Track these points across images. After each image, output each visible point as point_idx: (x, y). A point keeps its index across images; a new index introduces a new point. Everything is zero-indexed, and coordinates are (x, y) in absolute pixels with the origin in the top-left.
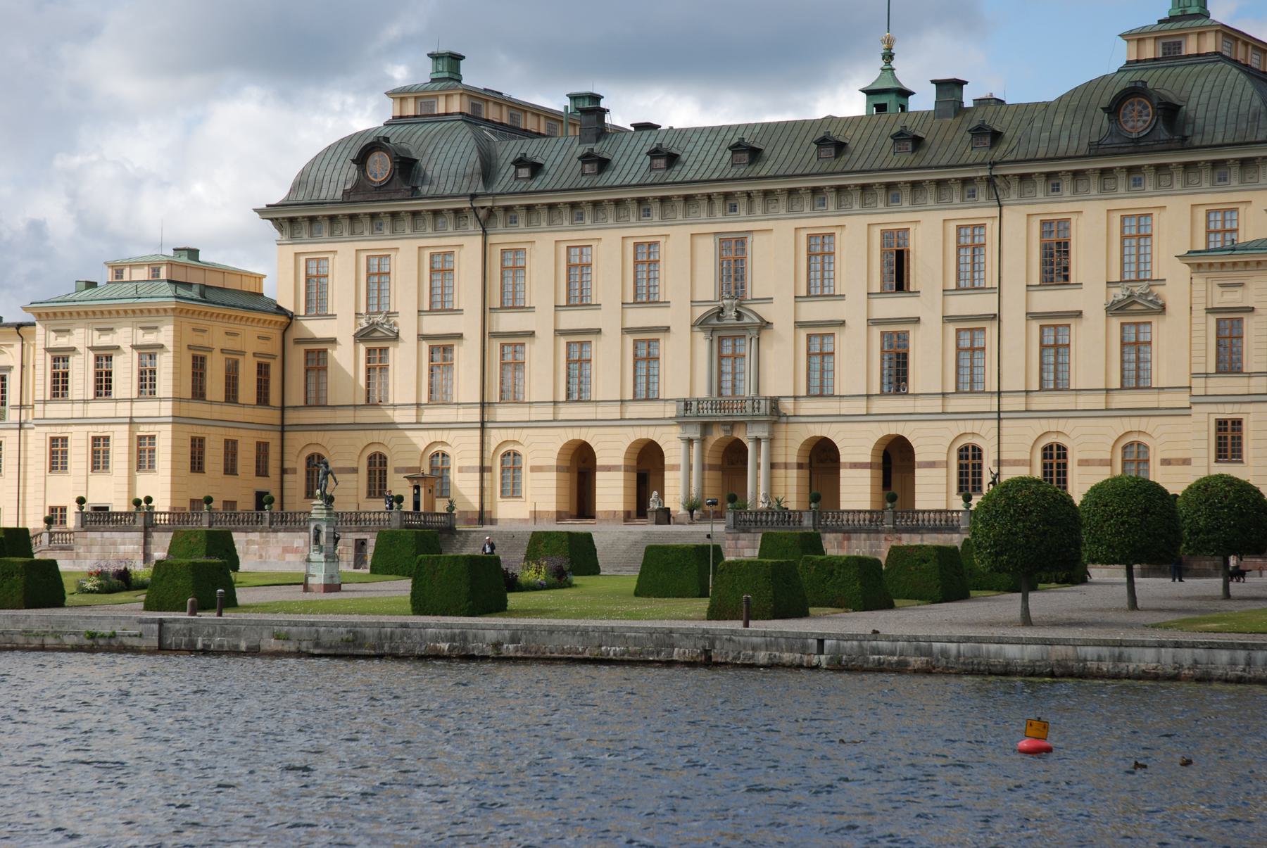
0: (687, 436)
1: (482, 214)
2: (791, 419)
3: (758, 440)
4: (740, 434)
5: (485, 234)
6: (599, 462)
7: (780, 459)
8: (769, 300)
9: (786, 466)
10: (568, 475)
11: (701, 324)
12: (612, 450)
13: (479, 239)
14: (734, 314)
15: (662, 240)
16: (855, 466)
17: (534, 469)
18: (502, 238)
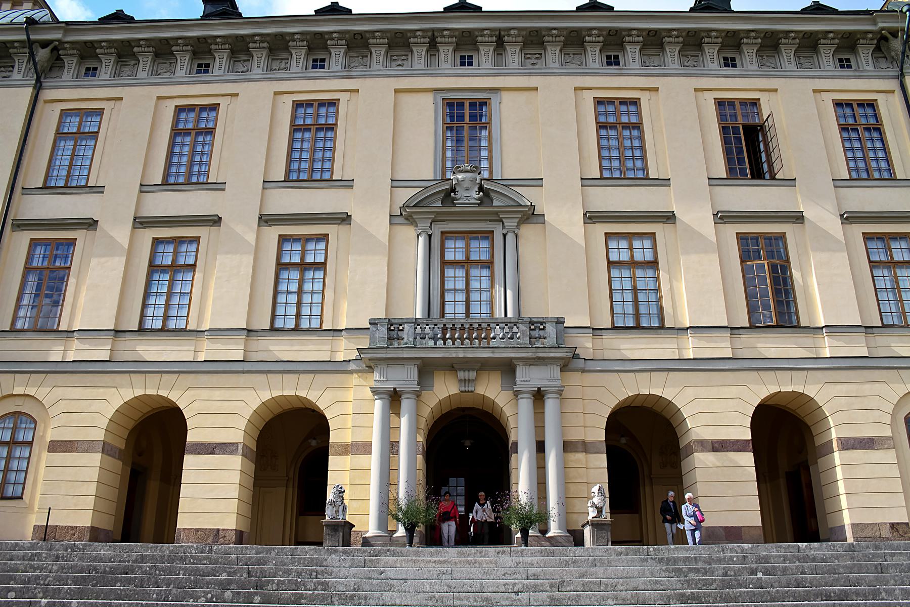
0: (390, 386)
1: (42, 55)
2: (590, 365)
3: (539, 396)
4: (491, 390)
5: (38, 87)
6: (191, 437)
7: (575, 435)
8: (537, 182)
9: (586, 447)
10: (119, 464)
11: (406, 215)
12: (222, 415)
13: (28, 92)
14: (475, 194)
15: (343, 98)
16: (719, 446)
17: (56, 447)
18: (67, 93)
